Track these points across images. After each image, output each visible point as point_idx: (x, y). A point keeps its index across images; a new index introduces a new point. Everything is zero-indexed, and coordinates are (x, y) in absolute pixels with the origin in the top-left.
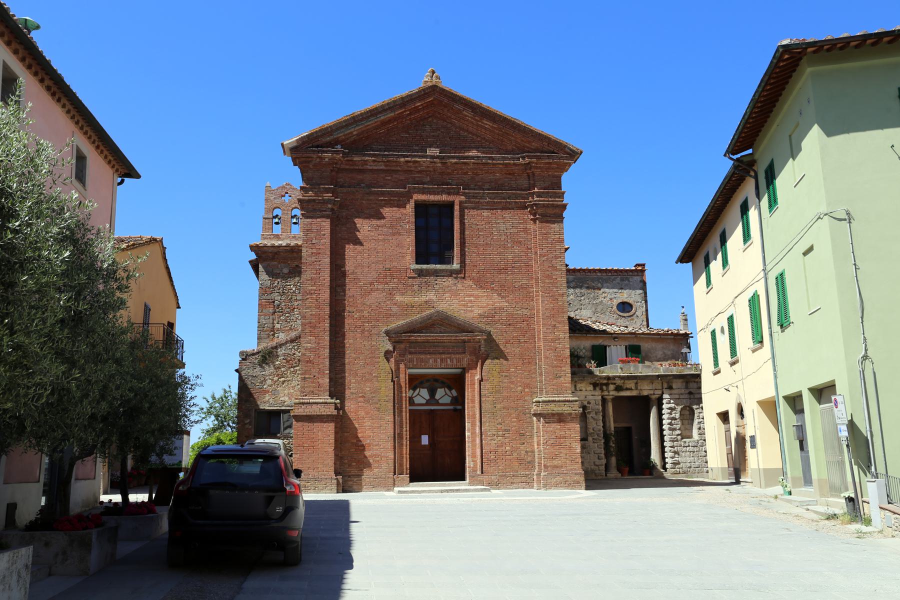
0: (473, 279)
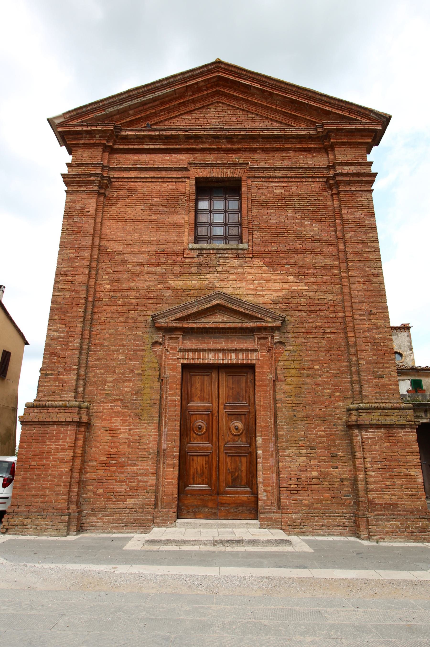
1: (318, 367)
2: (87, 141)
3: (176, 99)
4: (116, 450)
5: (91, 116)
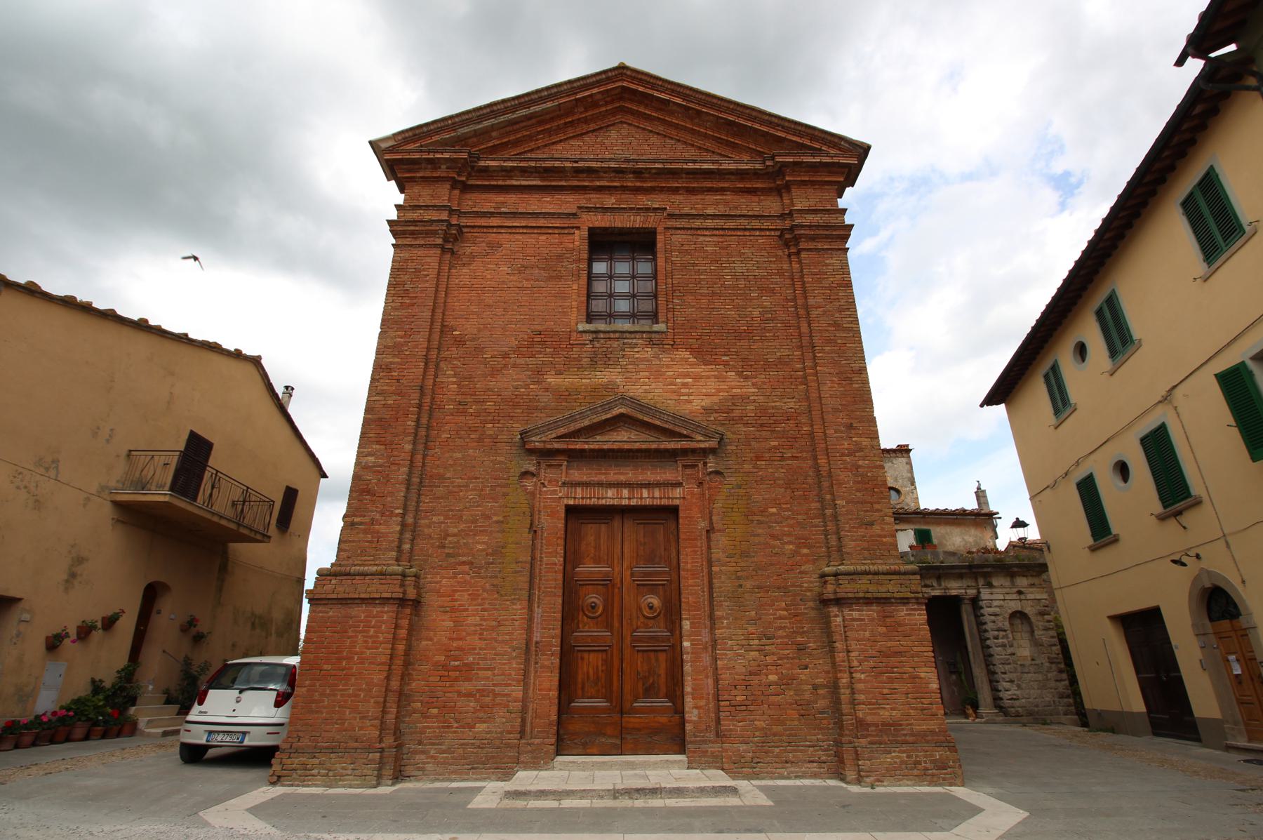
0: (690, 348)
1: (774, 510)
2: (428, 174)
3: (560, 117)
4: (460, 643)
5: (434, 139)
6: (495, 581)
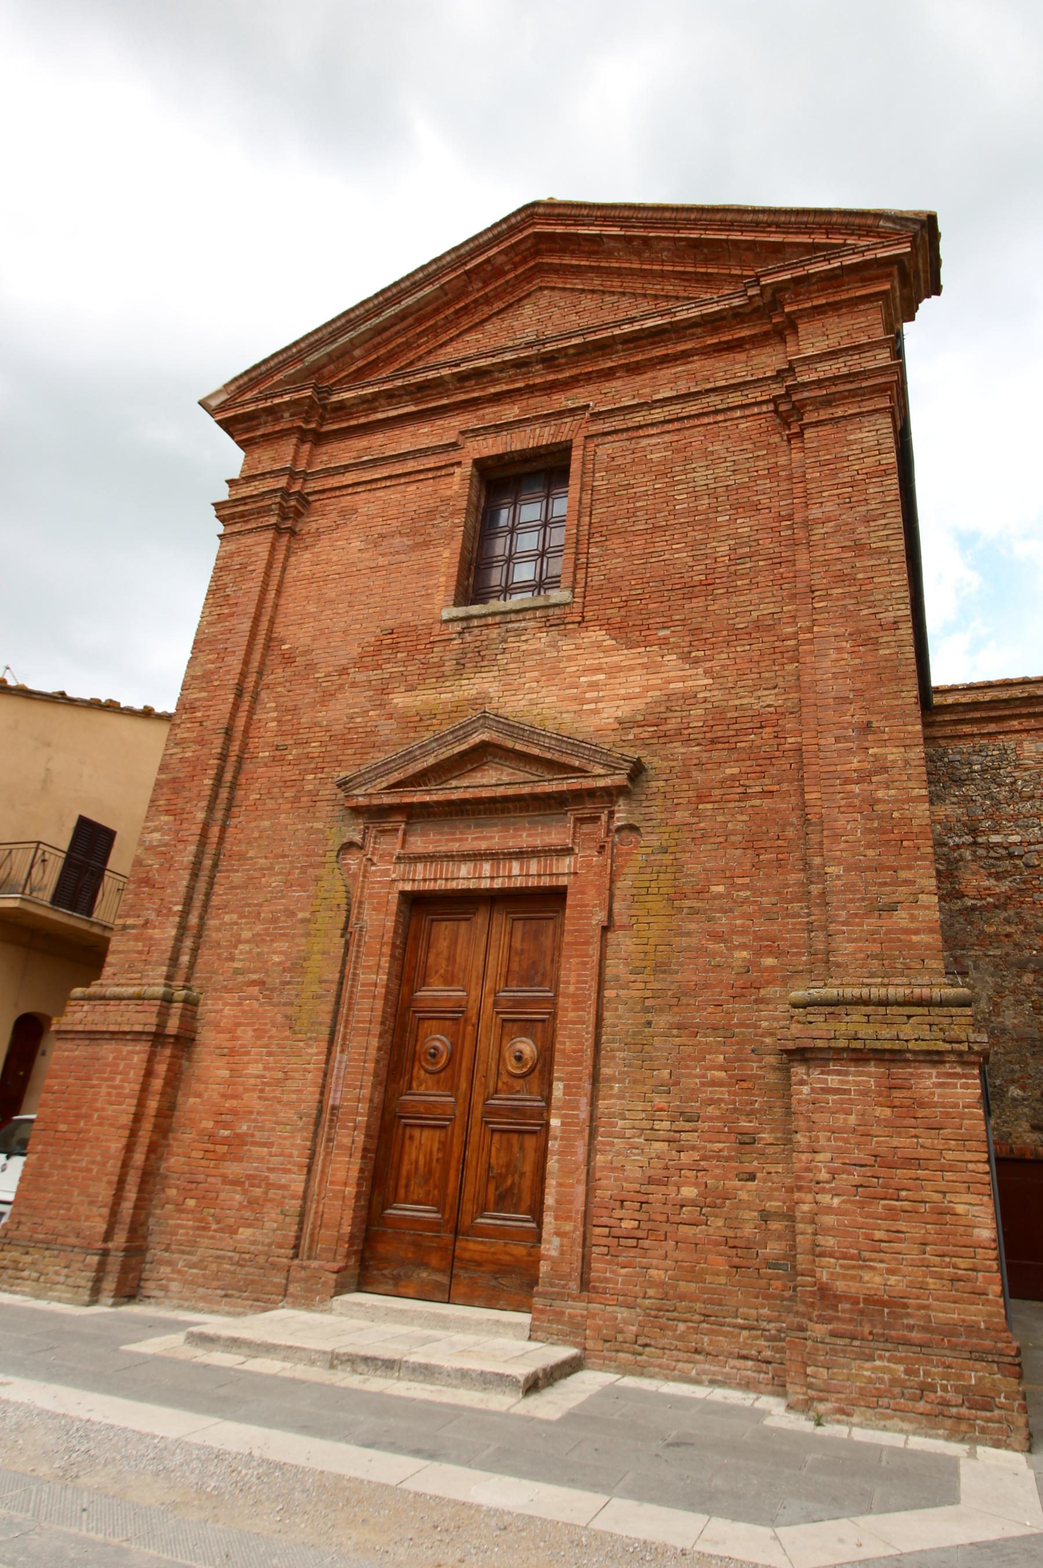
0: (607, 625)
1: (720, 889)
2: (269, 429)
3: (447, 304)
4: (234, 1102)
5: (276, 379)
6: (290, 1011)
